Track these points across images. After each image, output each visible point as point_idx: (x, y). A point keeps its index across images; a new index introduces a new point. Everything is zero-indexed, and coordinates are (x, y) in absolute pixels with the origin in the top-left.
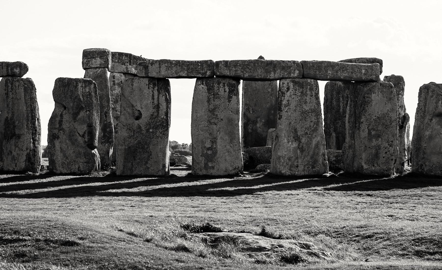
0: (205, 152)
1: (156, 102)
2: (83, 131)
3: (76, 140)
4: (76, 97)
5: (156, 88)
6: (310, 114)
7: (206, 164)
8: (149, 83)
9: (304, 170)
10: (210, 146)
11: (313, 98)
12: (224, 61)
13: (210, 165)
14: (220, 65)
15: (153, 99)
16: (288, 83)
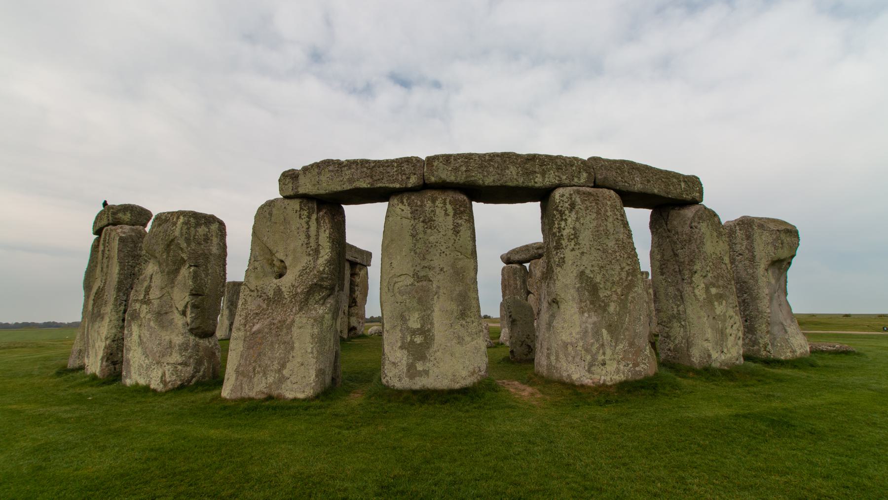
0: (409, 339)
1: (313, 243)
2: (183, 303)
3: (171, 322)
4: (173, 240)
5: (314, 216)
6: (618, 254)
7: (411, 367)
8: (301, 208)
9: (618, 371)
10: (419, 326)
11: (619, 224)
12: (443, 156)
13: (420, 367)
14: (435, 164)
15: (308, 237)
16: (571, 195)
